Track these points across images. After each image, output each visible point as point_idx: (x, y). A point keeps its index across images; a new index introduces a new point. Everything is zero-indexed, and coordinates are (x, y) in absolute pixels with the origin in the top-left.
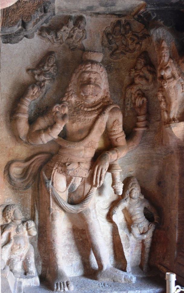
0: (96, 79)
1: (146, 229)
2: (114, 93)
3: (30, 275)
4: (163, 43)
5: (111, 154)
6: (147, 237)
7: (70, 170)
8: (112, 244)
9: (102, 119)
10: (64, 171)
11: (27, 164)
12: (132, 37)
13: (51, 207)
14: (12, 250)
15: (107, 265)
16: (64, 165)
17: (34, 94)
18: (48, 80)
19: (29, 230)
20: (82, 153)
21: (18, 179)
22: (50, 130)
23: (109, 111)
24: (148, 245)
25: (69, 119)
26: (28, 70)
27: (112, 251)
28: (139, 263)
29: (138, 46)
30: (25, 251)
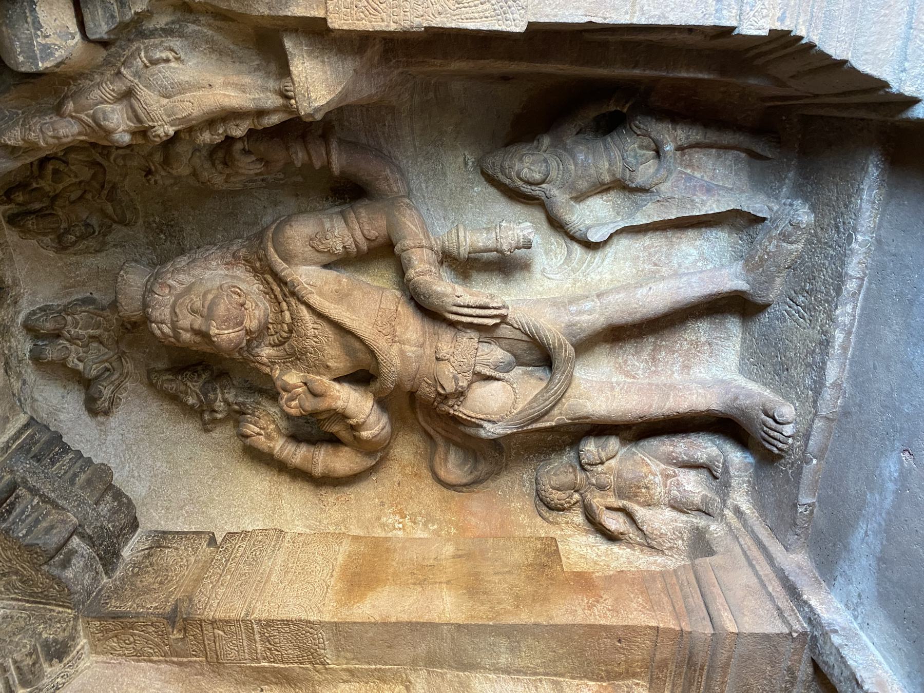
0: (193, 311)
1: (646, 141)
3: (719, 470)
4: (9, 143)
5: (411, 273)
6: (671, 137)
7: (457, 384)
8: (669, 234)
10: (460, 394)
13: (554, 424)
15: (736, 277)
16: (446, 397)
17: (262, 432)
18: (223, 393)
19: (604, 459)
20: (410, 350)
21: (475, 468)
22: (352, 422)
23: (285, 265)
24: (696, 135)
25: (319, 374)
26: (207, 431)
27: (691, 233)
28: (743, 155)
30: (653, 467)
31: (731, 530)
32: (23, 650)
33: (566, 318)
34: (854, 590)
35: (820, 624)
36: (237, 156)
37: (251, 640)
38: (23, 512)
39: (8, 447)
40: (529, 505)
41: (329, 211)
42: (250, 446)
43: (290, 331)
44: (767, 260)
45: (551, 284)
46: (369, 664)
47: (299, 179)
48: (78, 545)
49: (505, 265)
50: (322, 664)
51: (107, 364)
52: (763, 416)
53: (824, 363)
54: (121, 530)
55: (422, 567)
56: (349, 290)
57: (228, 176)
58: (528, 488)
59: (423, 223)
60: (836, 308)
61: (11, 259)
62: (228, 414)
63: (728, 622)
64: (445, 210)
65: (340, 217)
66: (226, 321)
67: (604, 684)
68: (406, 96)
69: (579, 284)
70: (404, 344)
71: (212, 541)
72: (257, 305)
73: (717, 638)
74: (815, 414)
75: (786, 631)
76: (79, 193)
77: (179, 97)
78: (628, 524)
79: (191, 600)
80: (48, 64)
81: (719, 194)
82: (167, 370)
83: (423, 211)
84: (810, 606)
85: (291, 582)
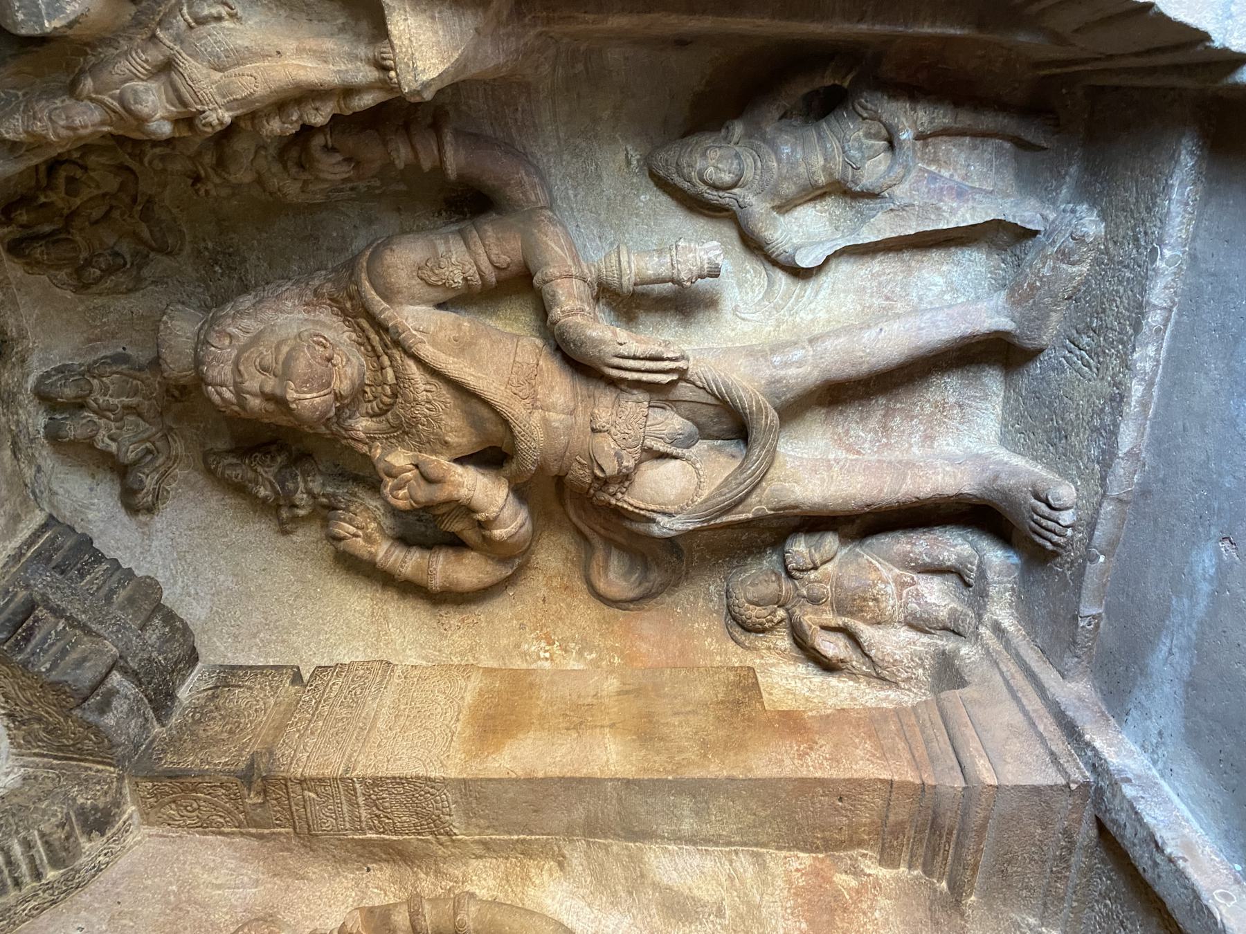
0: (264, 369)
1: (876, 127)
2: (317, 239)
3: (973, 575)
4: (7, 136)
5: (556, 313)
6: (909, 120)
7: (620, 464)
8: (906, 256)
9: (422, 342)
10: (625, 478)
11: (596, 540)
12: (63, 188)
13: (750, 516)
14: (879, 623)
15: (998, 313)
16: (605, 482)
17: (360, 533)
18: (306, 482)
19: (818, 562)
20: (556, 418)
23: (385, 305)
24: (943, 117)
25: (434, 452)
26: (285, 533)
27: (935, 255)
28: (1007, 145)
29: (92, 160)
30: (884, 573)
31: (988, 653)
32: (53, 820)
33: (767, 373)
34: (1153, 726)
35: (1108, 771)
36: (317, 153)
37: (353, 804)
38: (44, 640)
39: (22, 555)
40: (718, 626)
41: (444, 230)
42: (344, 552)
43: (395, 395)
44: (1039, 288)
45: (747, 327)
46: (510, 833)
47: (403, 187)
48: (120, 683)
49: (684, 302)
50: (447, 834)
51: (148, 444)
52: (1033, 501)
53: (1116, 426)
54: (176, 664)
55: (576, 707)
56: (472, 337)
57: (306, 182)
58: (717, 603)
59: (572, 244)
60: (1134, 350)
61: (15, 303)
62: (314, 510)
63: (984, 771)
64: (601, 226)
65: (458, 238)
66: (308, 381)
67: (821, 856)
68: (546, 69)
69: (783, 327)
70: (549, 412)
71: (297, 678)
72: (348, 360)
73: (970, 792)
74: (1104, 495)
75: (1061, 781)
76: (104, 209)
77: (237, 70)
78: (850, 649)
79: (271, 754)
80: (57, 23)
81: (974, 199)
82: (229, 452)
83: (571, 227)
84: (1094, 749)
85: (404, 729)
